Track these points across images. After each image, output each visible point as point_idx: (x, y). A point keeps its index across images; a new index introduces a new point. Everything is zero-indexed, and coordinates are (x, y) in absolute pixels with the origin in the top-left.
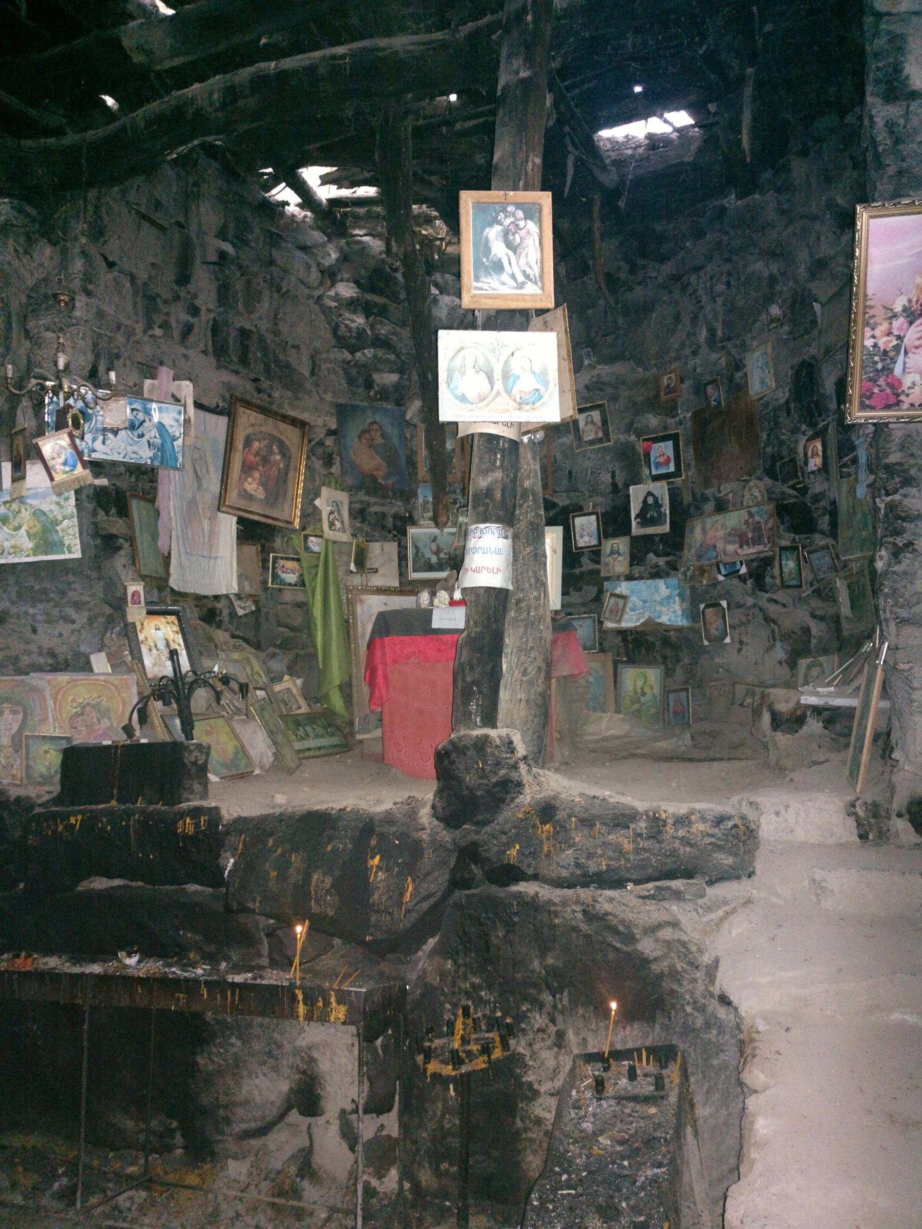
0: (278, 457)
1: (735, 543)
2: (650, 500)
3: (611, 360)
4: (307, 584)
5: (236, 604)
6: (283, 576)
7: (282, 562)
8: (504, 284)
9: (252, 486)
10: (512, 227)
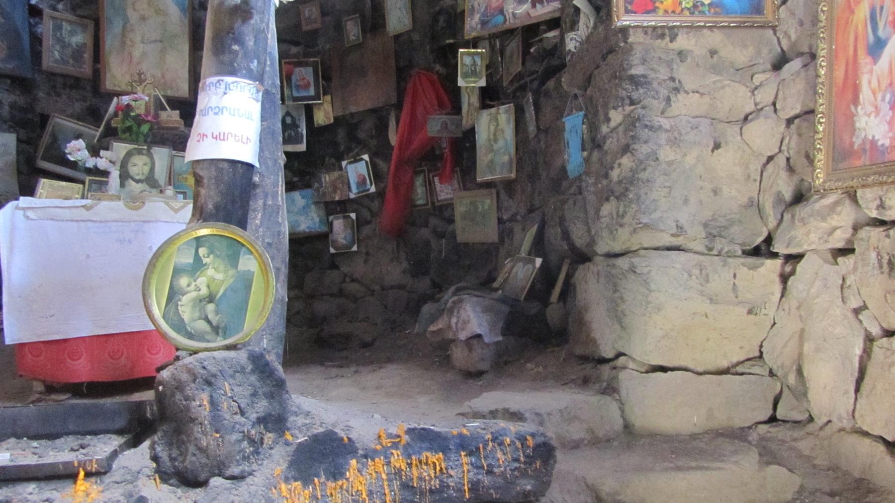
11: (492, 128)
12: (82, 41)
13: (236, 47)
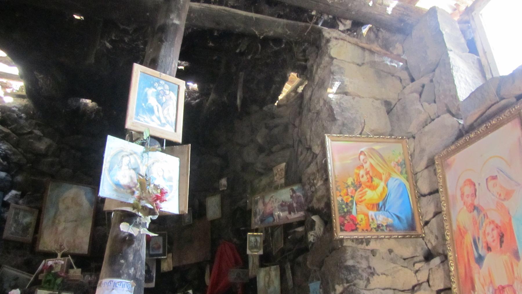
8: (153, 121)
10: (161, 92)
11: (267, 279)
13: (122, 261)
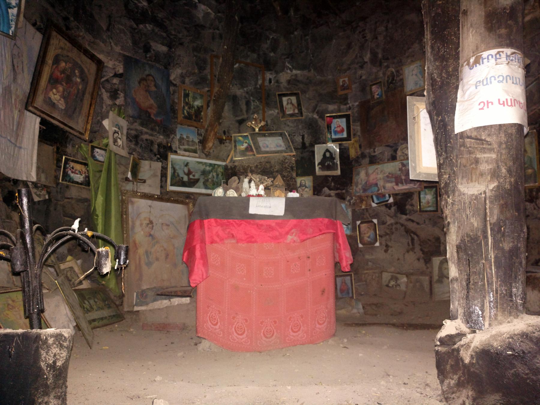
0: (78, 80)
1: (392, 182)
2: (328, 155)
3: (303, 68)
4: (92, 183)
5: (33, 191)
6: (72, 175)
7: (72, 164)
9: (55, 96)
12: (200, 105)
